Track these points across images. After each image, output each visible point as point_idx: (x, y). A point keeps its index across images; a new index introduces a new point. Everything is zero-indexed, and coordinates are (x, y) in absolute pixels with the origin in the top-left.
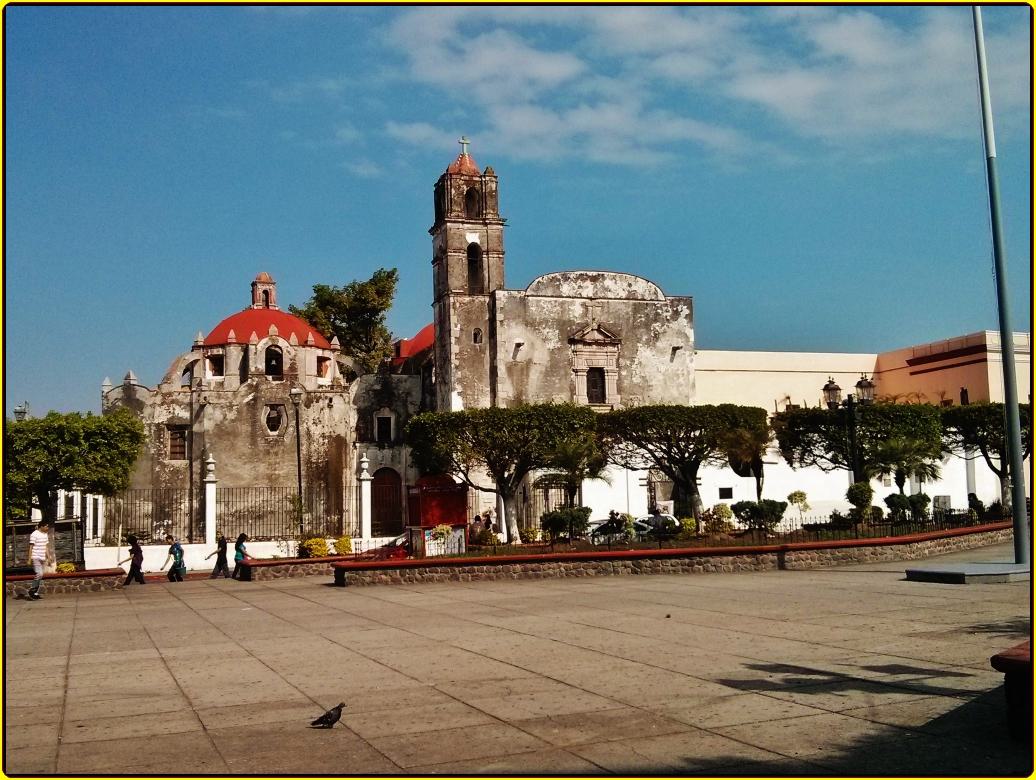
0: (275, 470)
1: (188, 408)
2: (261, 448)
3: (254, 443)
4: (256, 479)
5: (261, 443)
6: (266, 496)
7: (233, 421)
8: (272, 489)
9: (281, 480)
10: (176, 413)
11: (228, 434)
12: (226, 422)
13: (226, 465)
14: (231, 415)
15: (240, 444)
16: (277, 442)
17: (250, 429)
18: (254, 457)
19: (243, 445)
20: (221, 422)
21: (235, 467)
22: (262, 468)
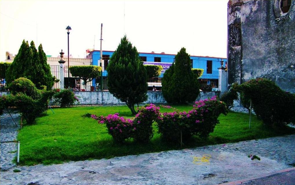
0: (282, 44)
1: (275, 10)
2: (273, 29)
3: (268, 26)
4: (269, 53)
5: (272, 23)
6: (276, 66)
7: (256, 12)
8: (280, 61)
9: (286, 52)
10: (237, 16)
11: (253, 22)
12: (252, 14)
13: (252, 45)
14: (255, 8)
15: (260, 28)
16: (285, 20)
17: (265, 15)
18: (267, 37)
19: (261, 29)
20: (250, 14)
21: (256, 45)
22: (273, 44)
